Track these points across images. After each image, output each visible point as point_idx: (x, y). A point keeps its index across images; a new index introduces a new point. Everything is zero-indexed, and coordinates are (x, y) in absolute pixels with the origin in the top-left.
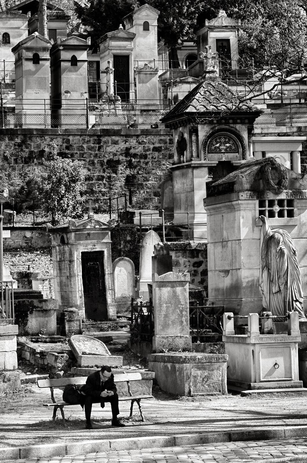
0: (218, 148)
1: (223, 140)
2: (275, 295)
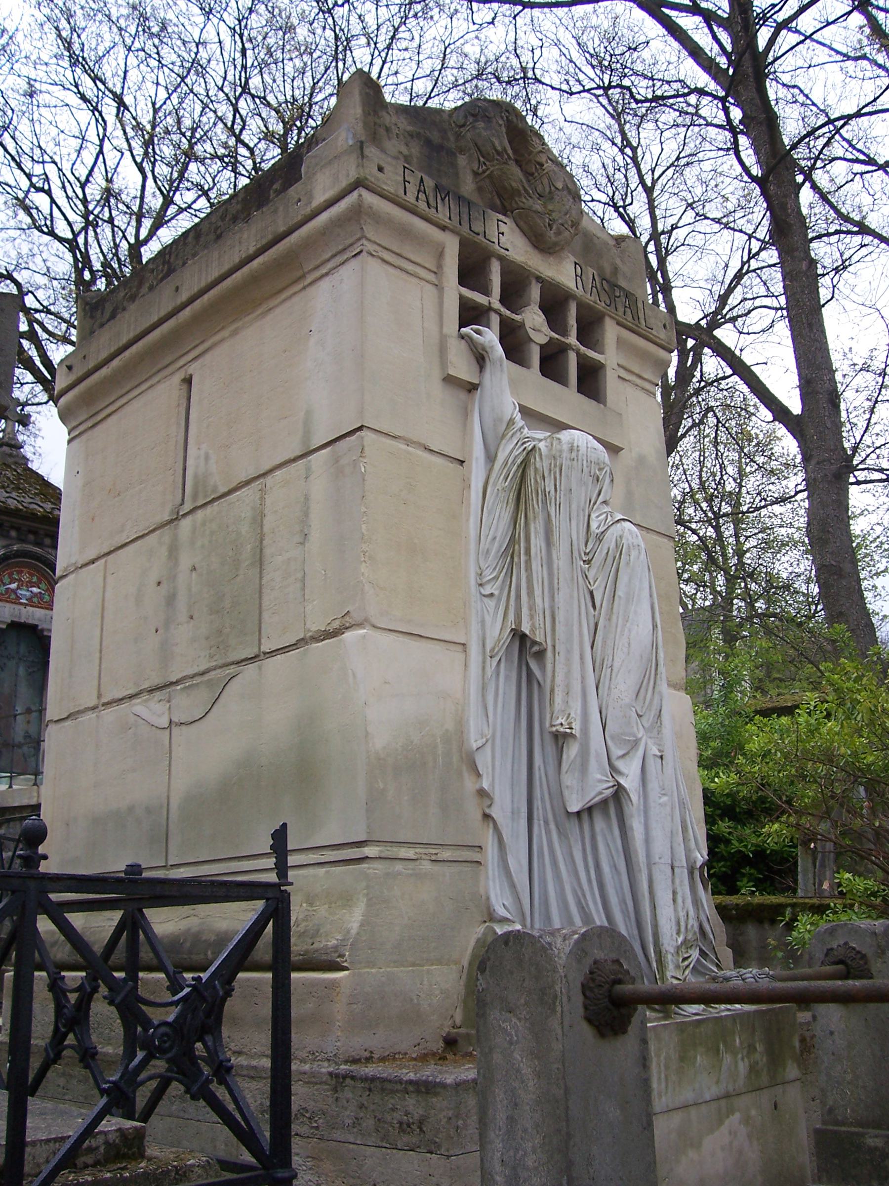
0: (14, 591)
1: (26, 577)
2: (573, 827)
